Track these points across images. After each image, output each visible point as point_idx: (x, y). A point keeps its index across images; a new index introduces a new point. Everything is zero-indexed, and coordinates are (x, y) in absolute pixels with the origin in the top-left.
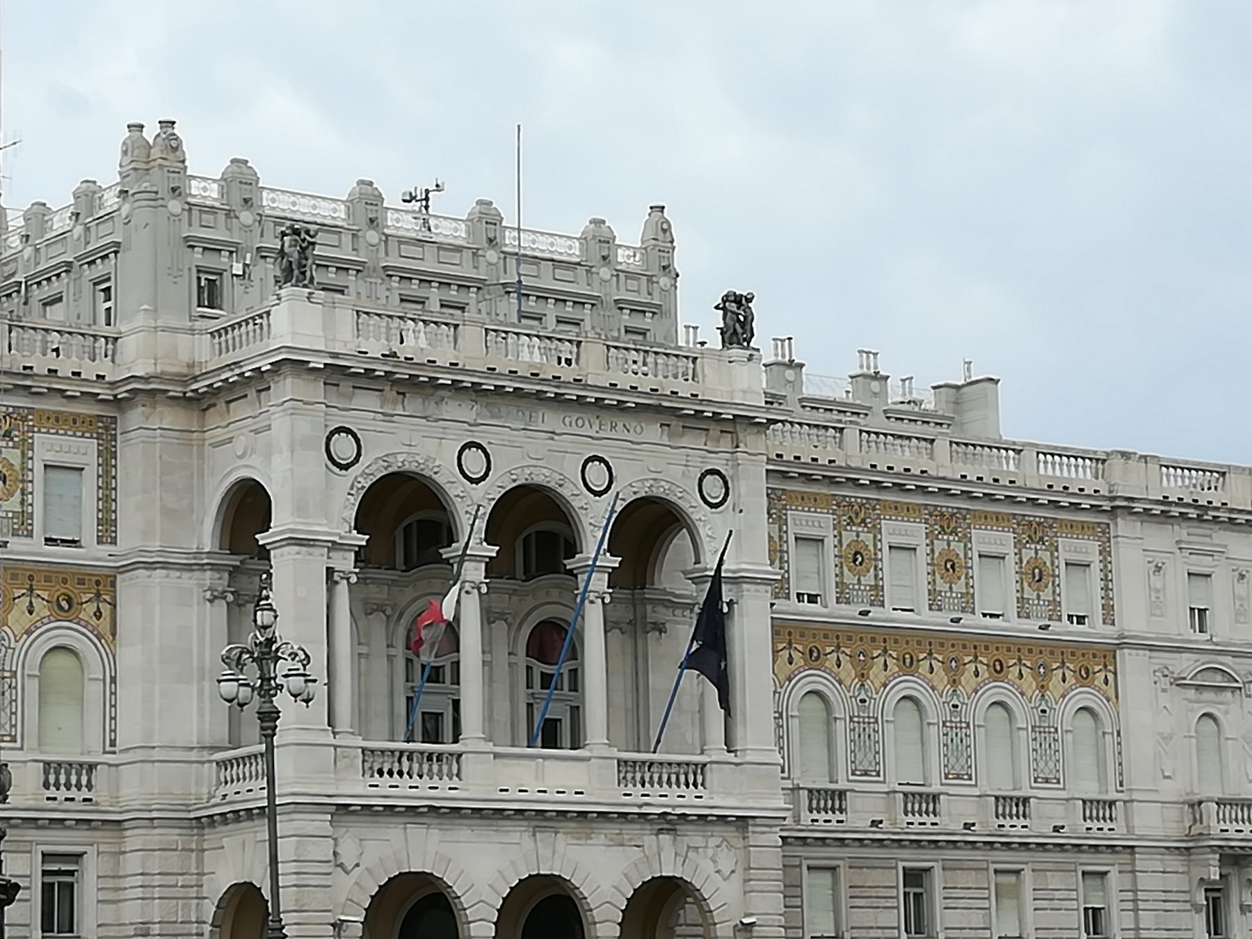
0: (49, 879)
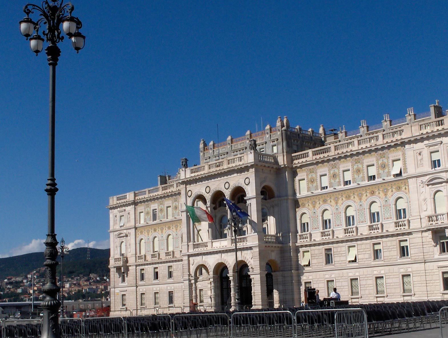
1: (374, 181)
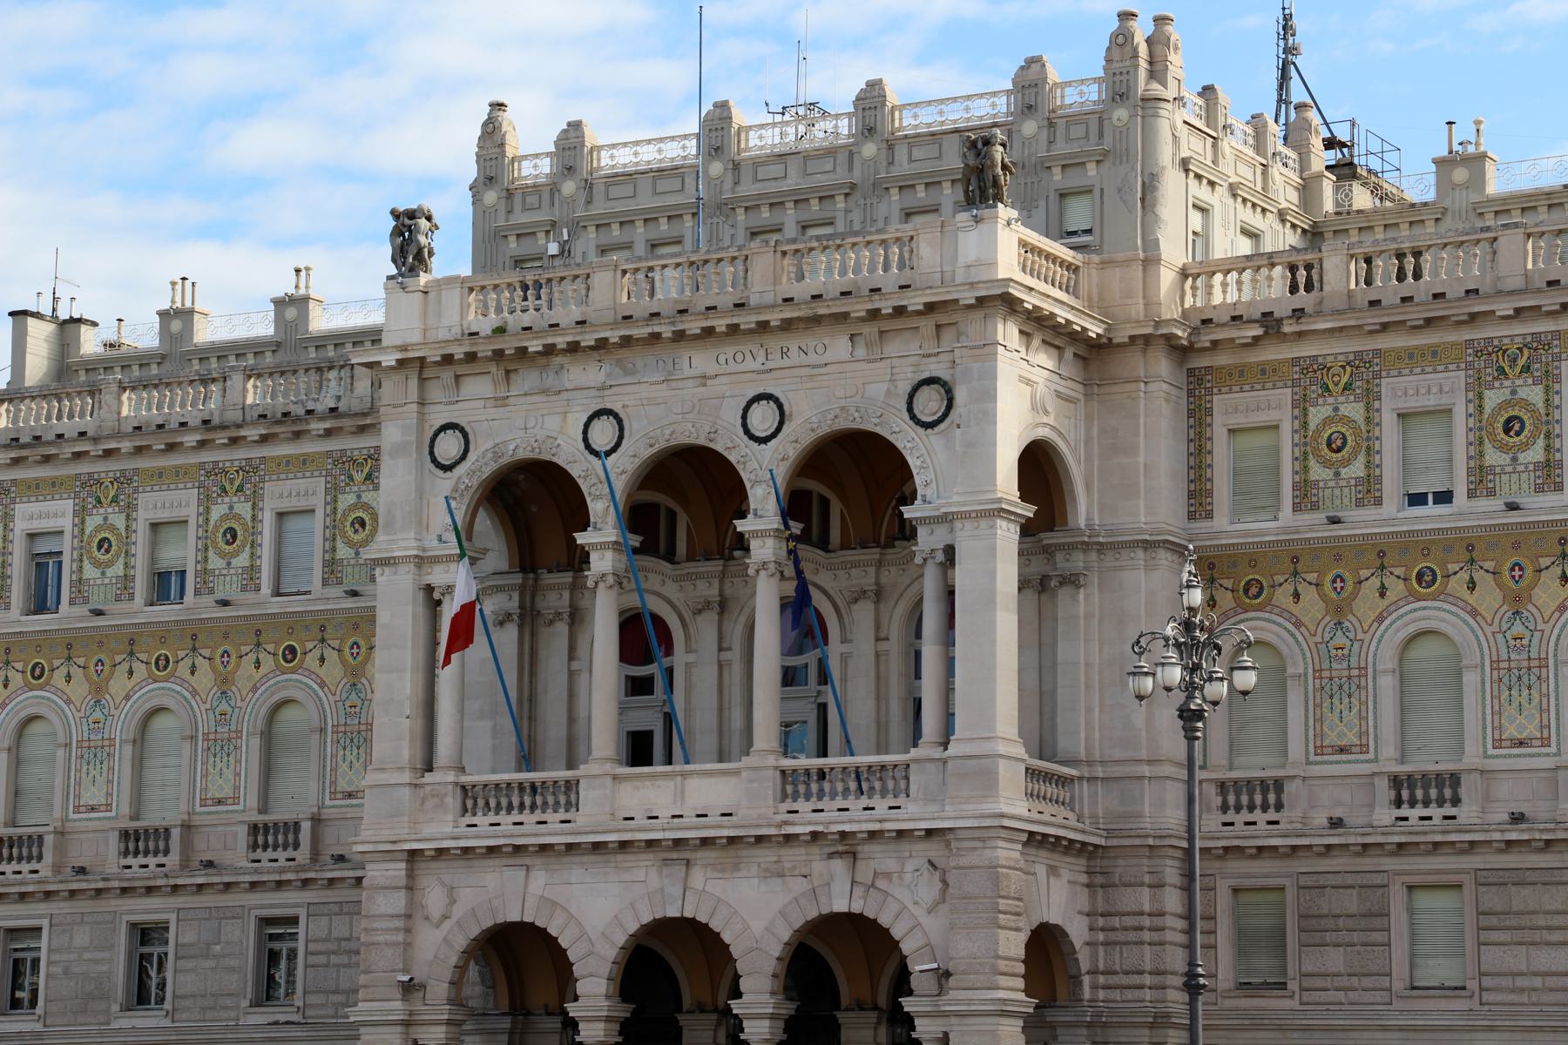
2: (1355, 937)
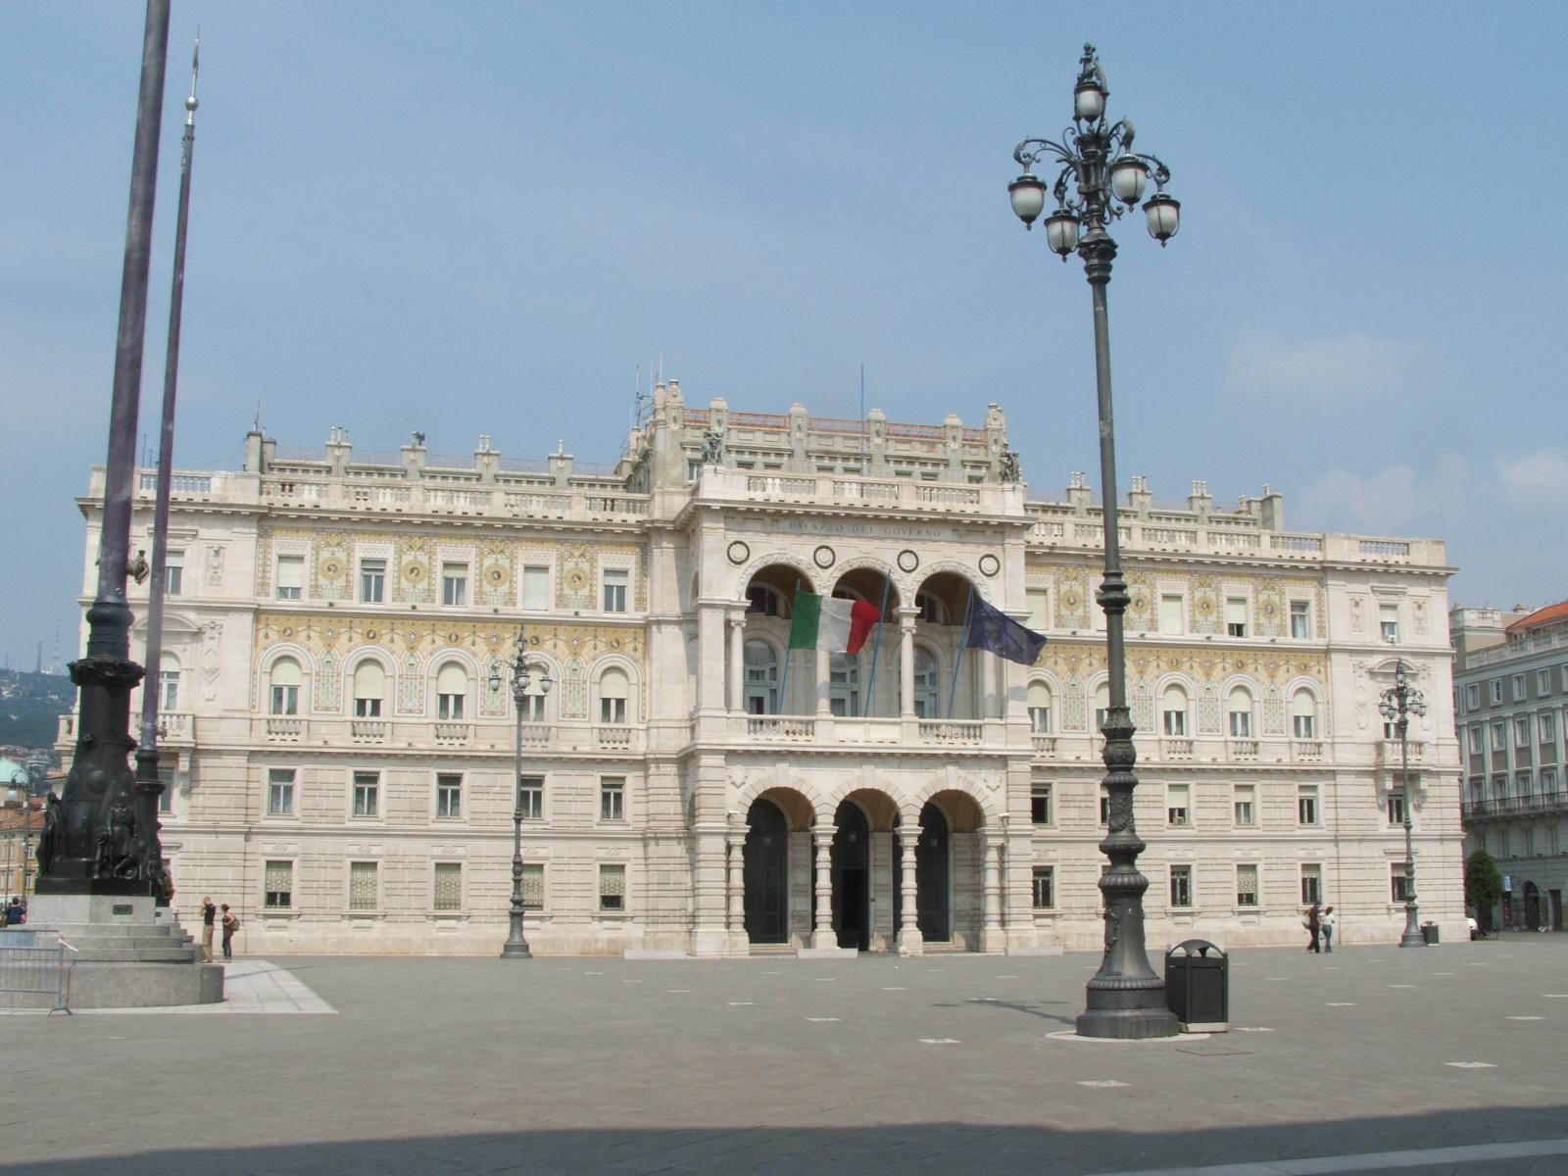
0: (606, 790)
1: (1239, 639)
2: (1083, 804)
